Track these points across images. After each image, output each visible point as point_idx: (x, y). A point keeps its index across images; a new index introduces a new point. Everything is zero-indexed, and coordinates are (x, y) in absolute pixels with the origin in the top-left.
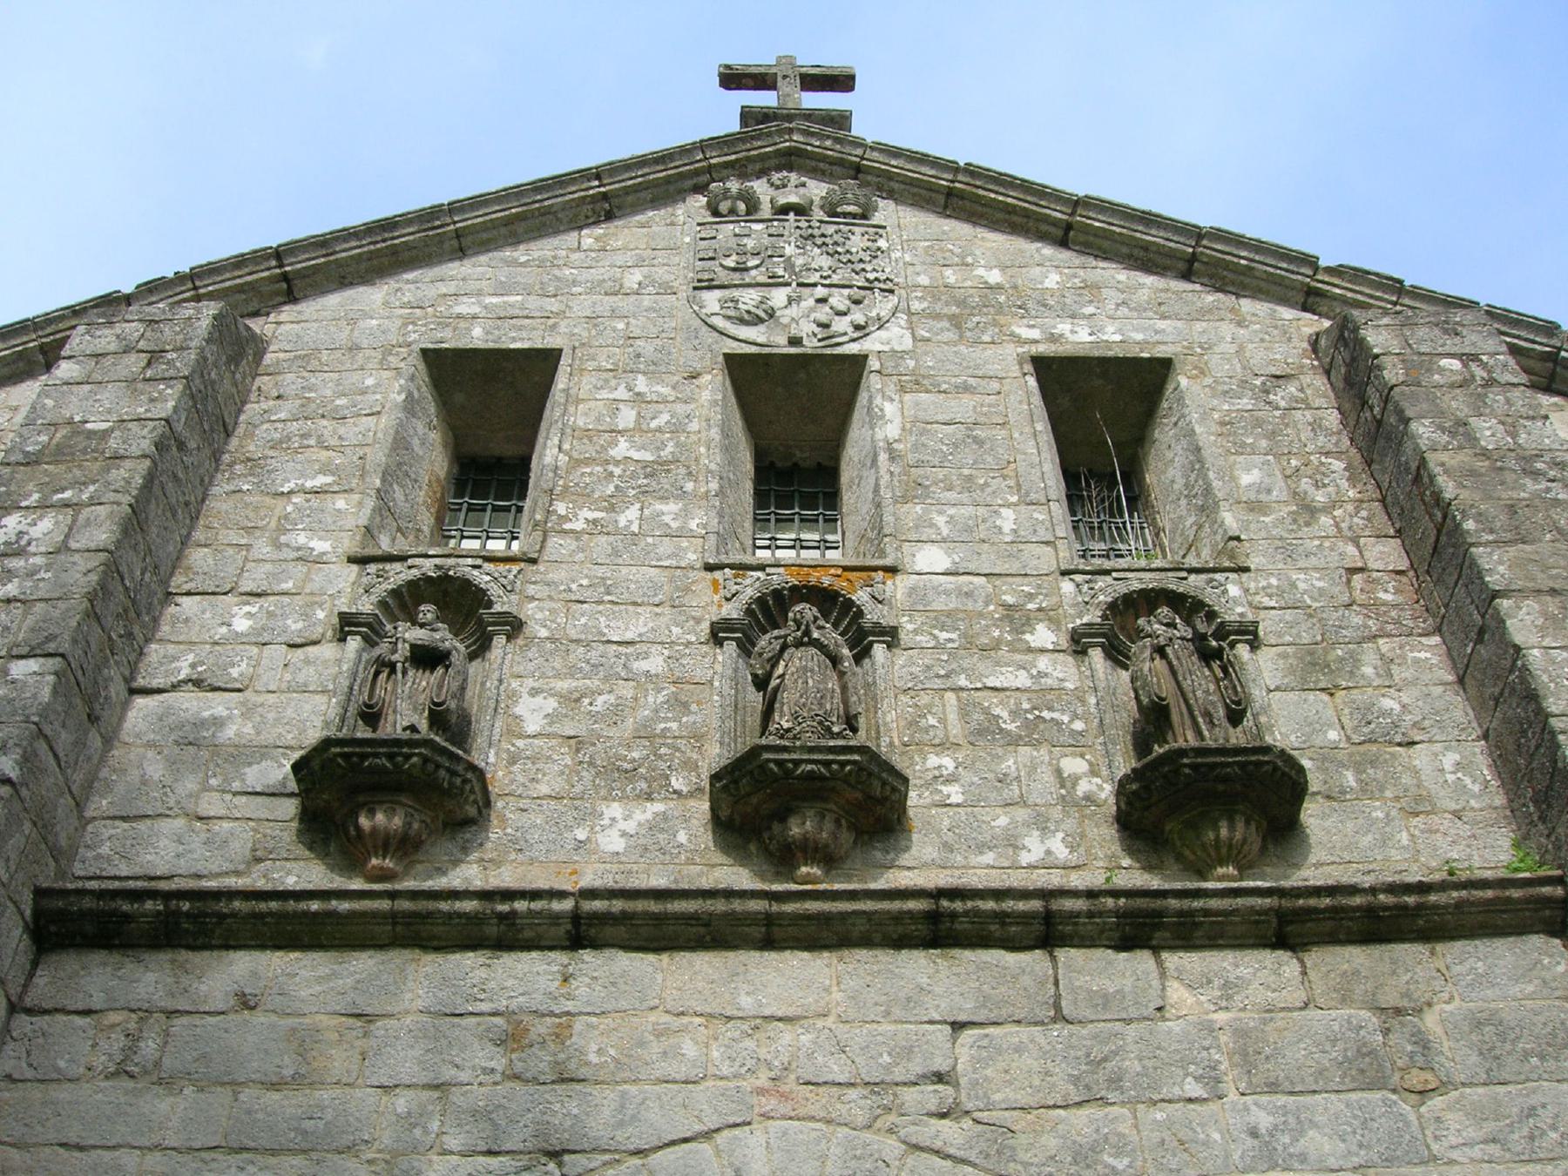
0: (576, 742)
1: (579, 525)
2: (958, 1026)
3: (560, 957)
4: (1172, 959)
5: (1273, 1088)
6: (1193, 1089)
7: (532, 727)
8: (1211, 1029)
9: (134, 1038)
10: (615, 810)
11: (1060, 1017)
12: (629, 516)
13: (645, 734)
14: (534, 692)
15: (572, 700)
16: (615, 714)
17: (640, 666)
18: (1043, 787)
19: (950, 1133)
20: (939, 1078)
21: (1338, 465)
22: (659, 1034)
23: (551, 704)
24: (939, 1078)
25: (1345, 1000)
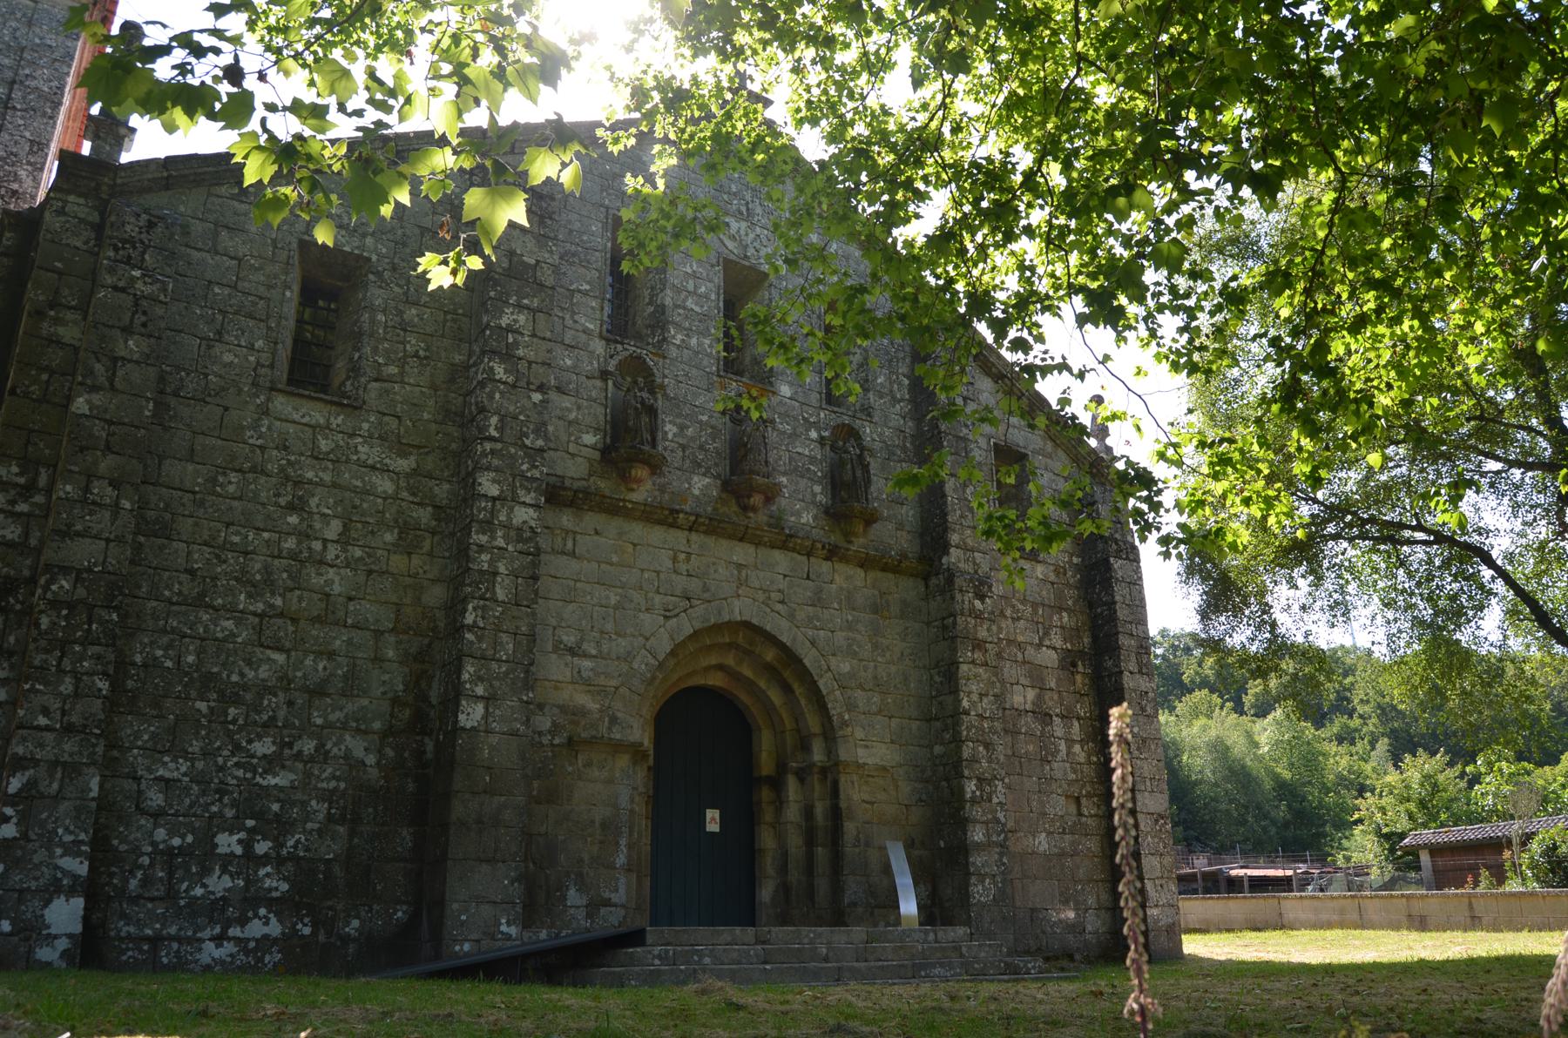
0: (684, 447)
1: (678, 342)
2: (785, 576)
3: (686, 533)
4: (837, 566)
5: (854, 609)
6: (836, 606)
7: (670, 436)
8: (841, 588)
9: (564, 539)
10: (696, 479)
11: (808, 578)
12: (694, 341)
13: (701, 447)
14: (670, 422)
15: (682, 428)
16: (692, 439)
17: (701, 417)
18: (808, 497)
19: (779, 607)
20: (779, 591)
21: (906, 382)
22: (714, 564)
23: (675, 429)
24: (779, 591)
25: (874, 587)
